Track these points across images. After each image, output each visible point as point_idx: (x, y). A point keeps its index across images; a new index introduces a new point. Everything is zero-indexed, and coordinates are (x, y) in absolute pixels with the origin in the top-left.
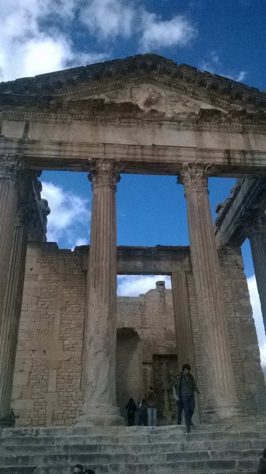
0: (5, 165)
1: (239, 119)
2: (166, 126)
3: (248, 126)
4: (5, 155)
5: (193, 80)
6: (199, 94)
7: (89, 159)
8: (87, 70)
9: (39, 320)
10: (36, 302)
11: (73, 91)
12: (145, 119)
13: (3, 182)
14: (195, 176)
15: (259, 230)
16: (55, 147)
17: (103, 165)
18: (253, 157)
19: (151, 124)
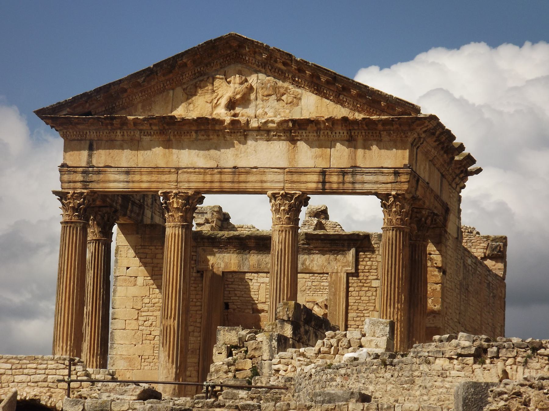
3: (355, 133)
9: (141, 343)
10: (136, 317)
11: (141, 92)
13: (70, 227)
16: (122, 177)
17: (175, 200)
18: (353, 179)
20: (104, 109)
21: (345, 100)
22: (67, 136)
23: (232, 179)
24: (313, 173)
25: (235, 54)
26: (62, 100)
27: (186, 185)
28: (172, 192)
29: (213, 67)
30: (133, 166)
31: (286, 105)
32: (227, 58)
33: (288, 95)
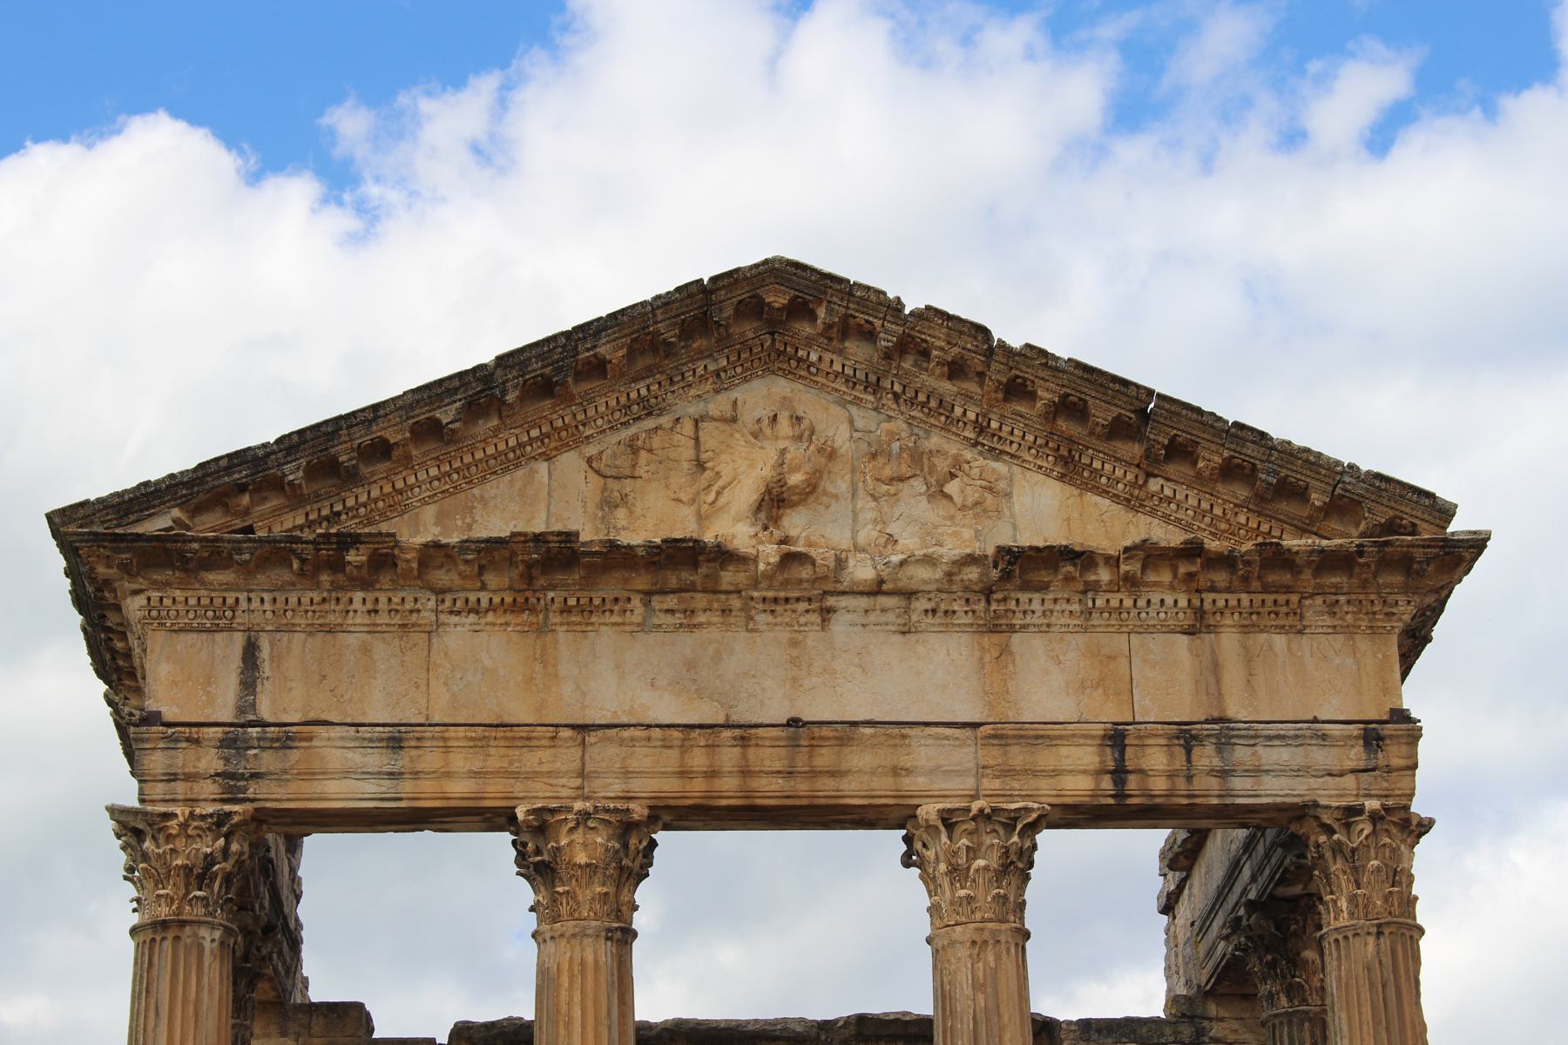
0: (179, 862)
1: (1175, 576)
2: (849, 617)
3: (1214, 601)
4: (173, 815)
5: (980, 369)
6: (1003, 434)
7: (520, 813)
8: (499, 372)
12: (756, 594)
14: (968, 869)
15: (1304, 1001)
16: (376, 759)
17: (578, 836)
18: (1222, 759)
19: (786, 611)
20: (300, 520)
21: (1168, 492)
22: (164, 613)
23: (786, 762)
24: (1082, 741)
26: (156, 473)
27: (616, 787)
28: (569, 809)
30: (412, 721)
31: (959, 515)
33: (966, 479)
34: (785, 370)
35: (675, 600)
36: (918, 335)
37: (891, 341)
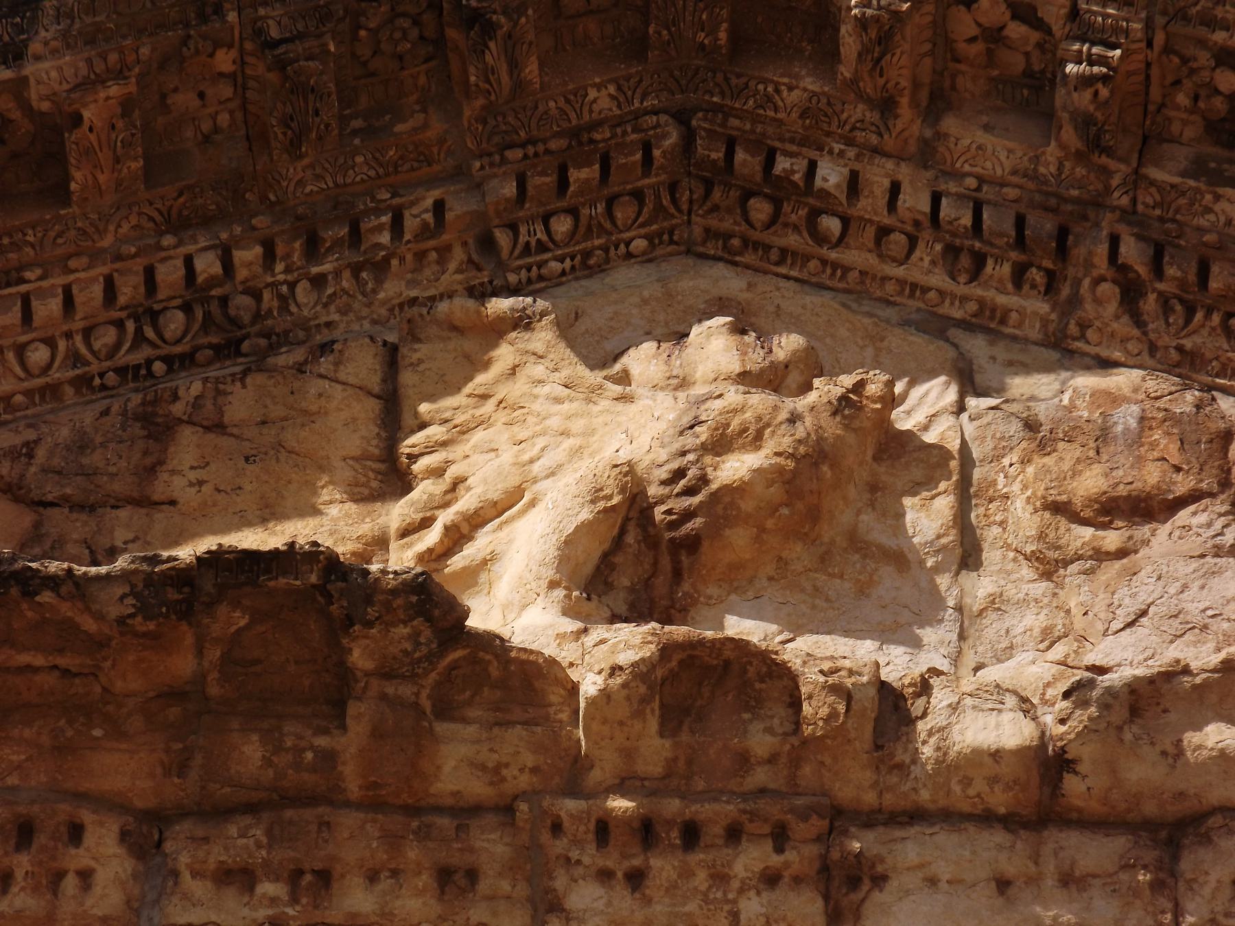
25: (673, 138)
29: (381, 268)
32: (577, 175)
34: (727, 236)
35: (259, 832)
36: (1202, 31)
37: (1102, 61)
